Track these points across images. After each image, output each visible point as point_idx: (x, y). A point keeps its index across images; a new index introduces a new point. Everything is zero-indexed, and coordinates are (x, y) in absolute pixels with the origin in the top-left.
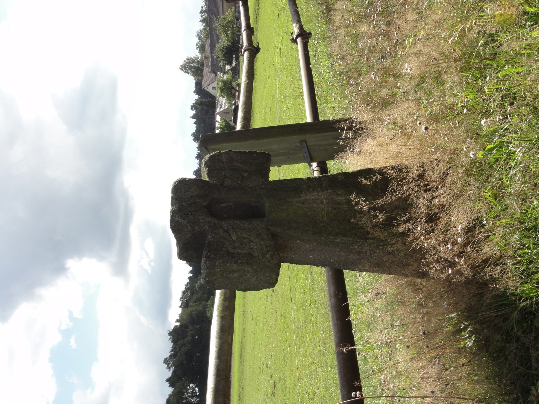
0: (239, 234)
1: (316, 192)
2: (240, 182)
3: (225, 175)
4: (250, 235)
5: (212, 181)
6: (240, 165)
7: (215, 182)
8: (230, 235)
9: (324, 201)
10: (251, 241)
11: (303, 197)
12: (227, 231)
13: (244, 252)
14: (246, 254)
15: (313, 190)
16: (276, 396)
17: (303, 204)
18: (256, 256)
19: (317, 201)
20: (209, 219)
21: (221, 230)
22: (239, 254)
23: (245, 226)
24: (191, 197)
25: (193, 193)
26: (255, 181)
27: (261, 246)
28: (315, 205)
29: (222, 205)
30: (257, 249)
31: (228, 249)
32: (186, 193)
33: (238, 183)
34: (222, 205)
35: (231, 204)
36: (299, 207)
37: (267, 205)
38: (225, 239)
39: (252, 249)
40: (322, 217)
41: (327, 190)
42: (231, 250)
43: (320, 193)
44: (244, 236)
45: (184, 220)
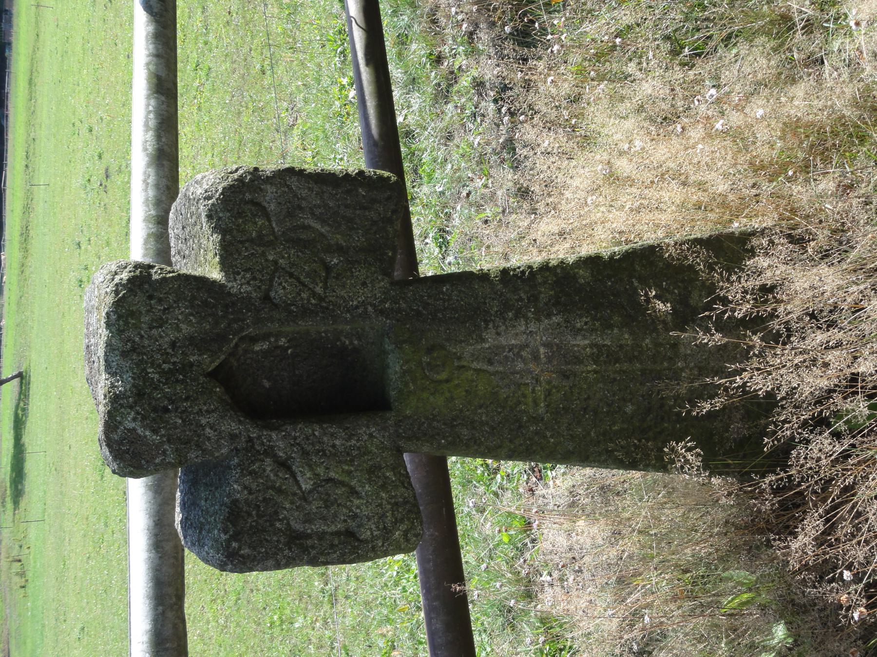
0: (320, 470)
1: (523, 322)
2: (319, 290)
3: (275, 262)
4: (349, 473)
5: (234, 287)
6: (318, 226)
7: (246, 288)
8: (293, 475)
9: (542, 350)
10: (353, 492)
11: (490, 339)
12: (284, 465)
13: (333, 528)
14: (338, 534)
15: (516, 317)
16: (110, 192)
17: (490, 362)
18: (366, 541)
19: (524, 353)
20: (231, 426)
21: (268, 461)
22: (321, 536)
23: (337, 442)
24: (173, 345)
25: (178, 329)
26: (364, 284)
27: (380, 505)
28: (520, 366)
29: (257, 348)
30: (369, 519)
31: (288, 524)
32: (154, 332)
33: (314, 294)
34: (257, 348)
35: (283, 341)
36: (478, 371)
37: (395, 367)
38: (280, 491)
39: (355, 516)
40: (536, 403)
41: (549, 316)
42: (297, 526)
43: (532, 327)
44: (332, 474)
45: (155, 431)
